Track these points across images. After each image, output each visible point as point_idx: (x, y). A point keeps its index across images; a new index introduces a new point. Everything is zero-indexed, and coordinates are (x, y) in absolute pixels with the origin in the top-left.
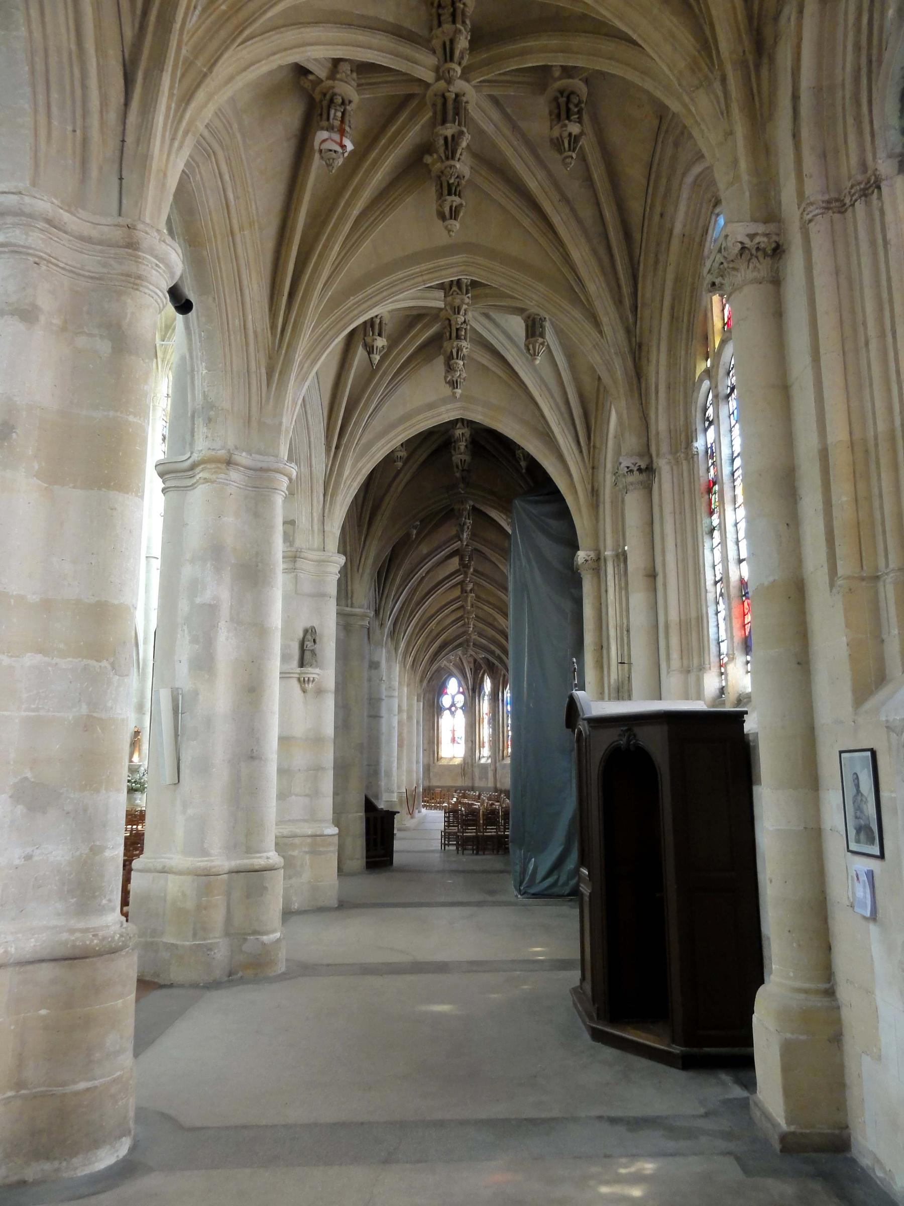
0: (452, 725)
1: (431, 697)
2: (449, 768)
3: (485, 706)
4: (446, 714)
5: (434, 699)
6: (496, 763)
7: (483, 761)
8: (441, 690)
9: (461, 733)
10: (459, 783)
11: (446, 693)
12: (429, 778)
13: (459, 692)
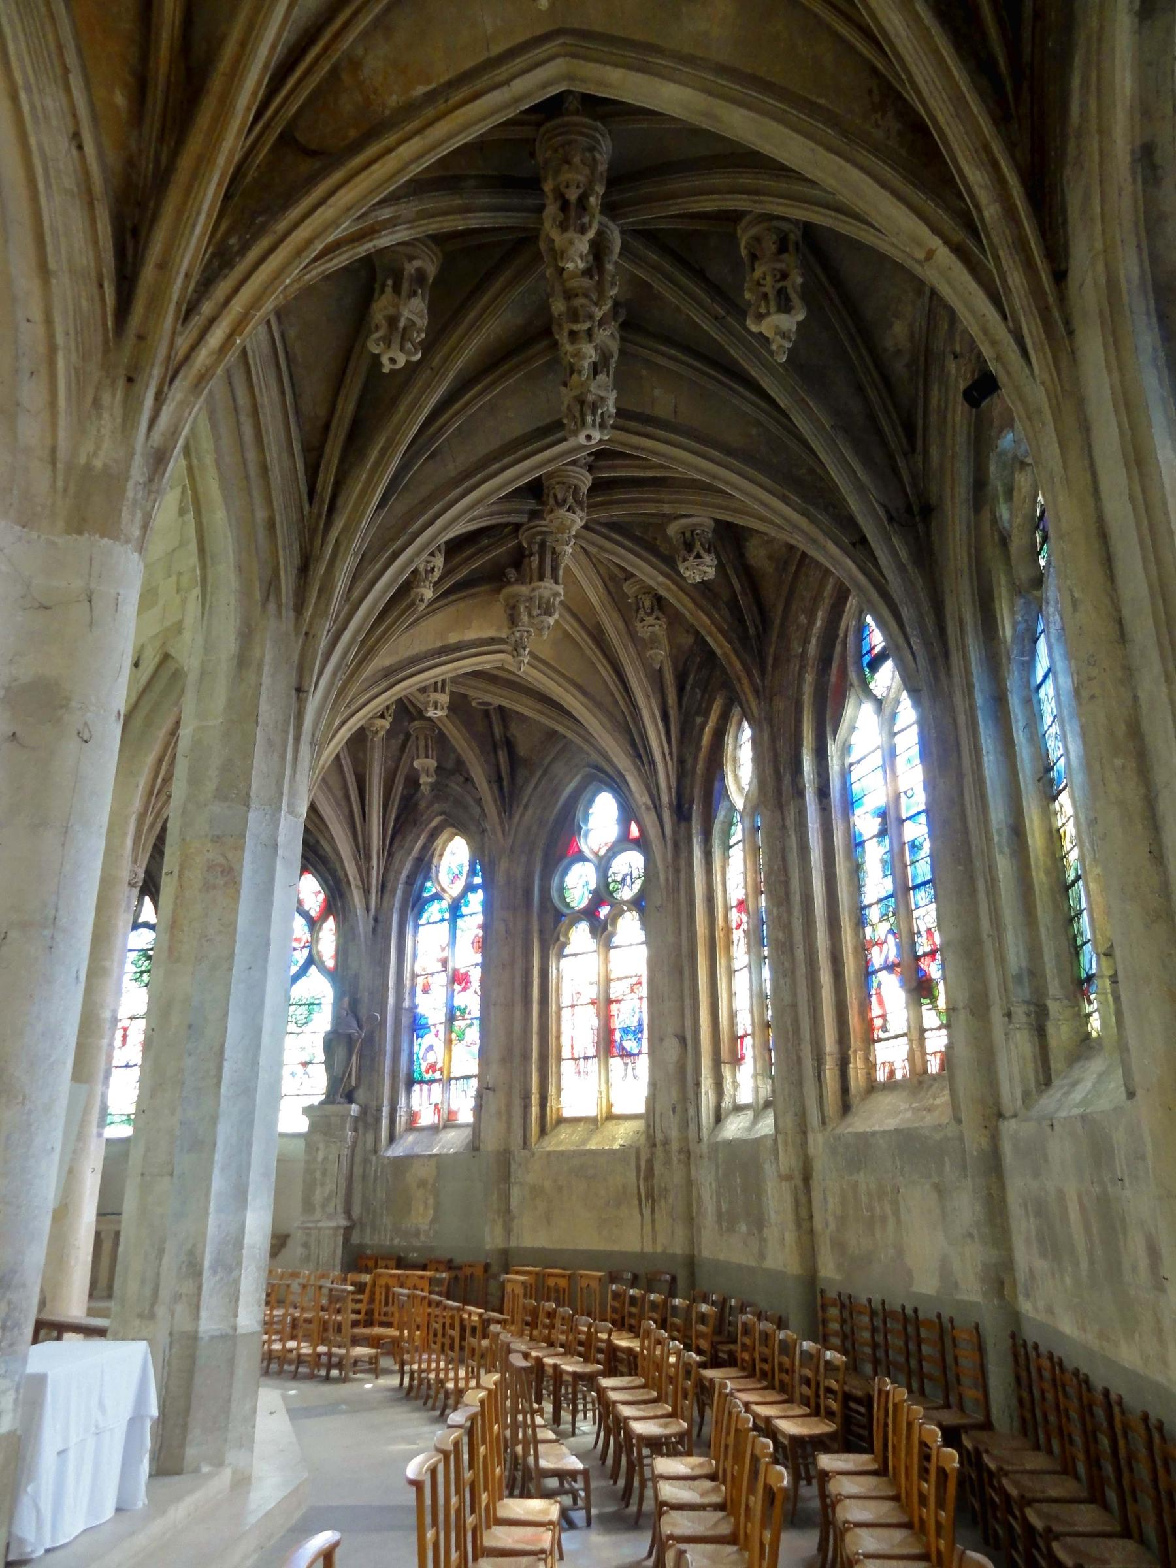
0: (602, 973)
1: (519, 873)
2: (586, 1166)
3: (735, 874)
4: (580, 936)
5: (529, 877)
6: (803, 1130)
7: (734, 1128)
8: (560, 845)
9: (632, 1010)
10: (631, 1237)
11: (581, 857)
12: (507, 1214)
13: (624, 842)
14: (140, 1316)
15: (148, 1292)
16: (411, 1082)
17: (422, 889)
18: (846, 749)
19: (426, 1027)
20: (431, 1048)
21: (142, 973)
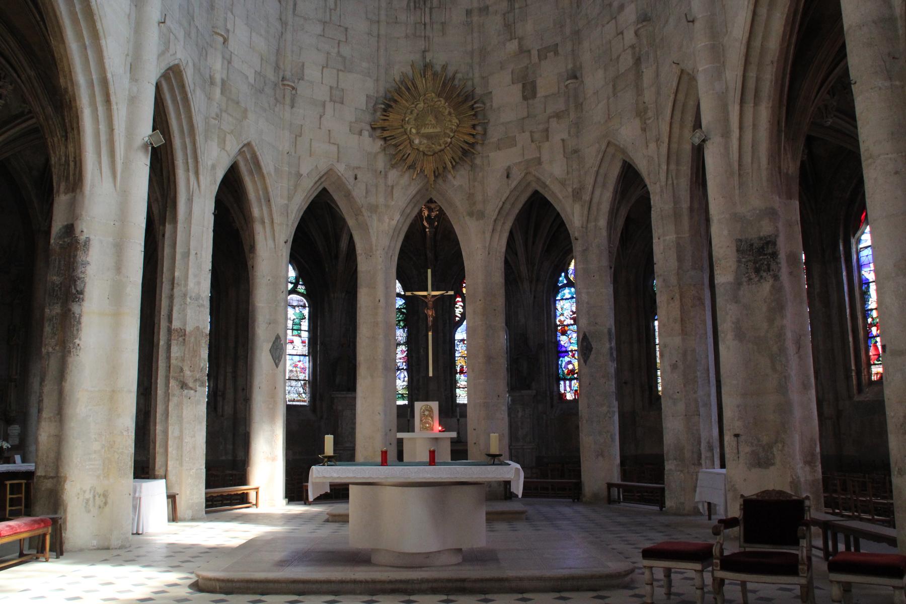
14: (694, 464)
15: (695, 456)
16: (558, 380)
17: (558, 281)
18: (859, 241)
19: (566, 352)
20: (570, 362)
21: (399, 321)
